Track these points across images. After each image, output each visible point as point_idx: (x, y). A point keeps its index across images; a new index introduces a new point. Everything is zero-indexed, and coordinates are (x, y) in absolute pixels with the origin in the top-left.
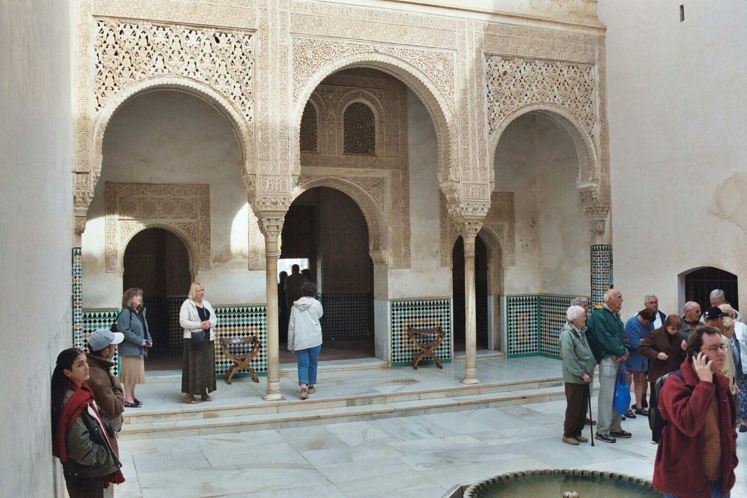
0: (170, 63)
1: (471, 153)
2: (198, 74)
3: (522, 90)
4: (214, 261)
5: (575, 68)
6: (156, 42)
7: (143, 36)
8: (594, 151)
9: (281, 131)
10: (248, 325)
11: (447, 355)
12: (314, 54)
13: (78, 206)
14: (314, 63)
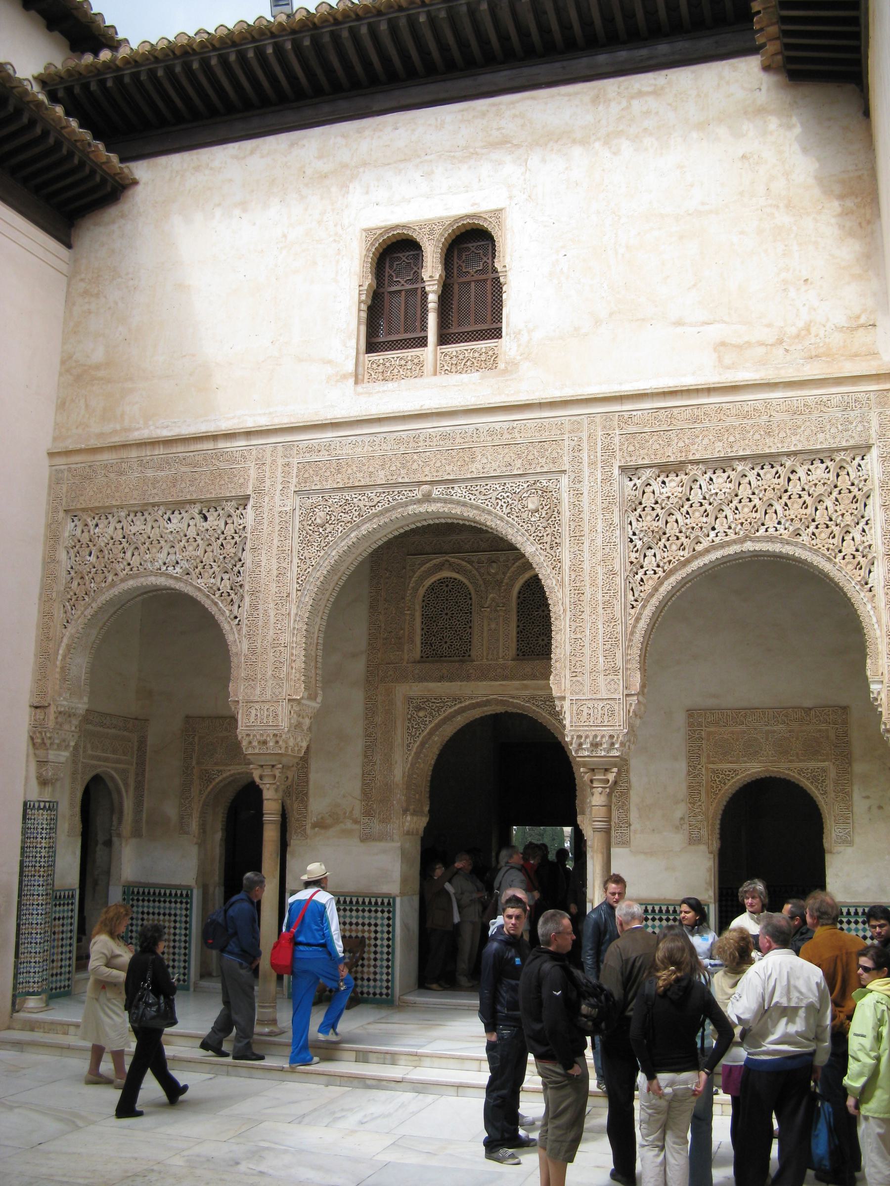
0: (148, 556)
1: (587, 645)
2: (178, 569)
4: (315, 826)
6: (133, 532)
7: (119, 526)
9: (274, 637)
10: (357, 924)
12: (328, 517)
13: (37, 749)
14: (328, 530)
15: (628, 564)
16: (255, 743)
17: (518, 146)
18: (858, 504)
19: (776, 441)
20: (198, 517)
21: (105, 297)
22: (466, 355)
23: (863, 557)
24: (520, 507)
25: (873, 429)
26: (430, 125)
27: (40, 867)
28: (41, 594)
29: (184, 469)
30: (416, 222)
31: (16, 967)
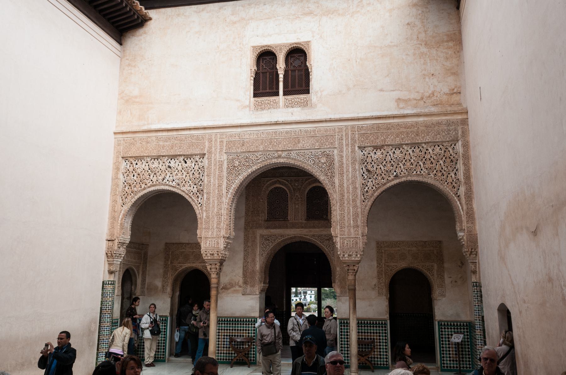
1: (346, 216)
2: (174, 183)
3: (392, 168)
4: (222, 289)
5: (441, 146)
6: (153, 167)
7: (147, 164)
8: (460, 208)
9: (217, 211)
10: (241, 330)
11: (385, 363)
12: (239, 163)
13: (109, 258)
14: (239, 169)
15: (362, 185)
16: (209, 255)
17: (316, 15)
18: (453, 163)
19: (420, 138)
20: (183, 162)
21: (138, 68)
22: (295, 100)
23: (456, 183)
24: (318, 161)
25: (460, 134)
26: (279, 4)
27: (109, 309)
28: (111, 192)
29: (176, 142)
30: (274, 44)
31: (97, 355)
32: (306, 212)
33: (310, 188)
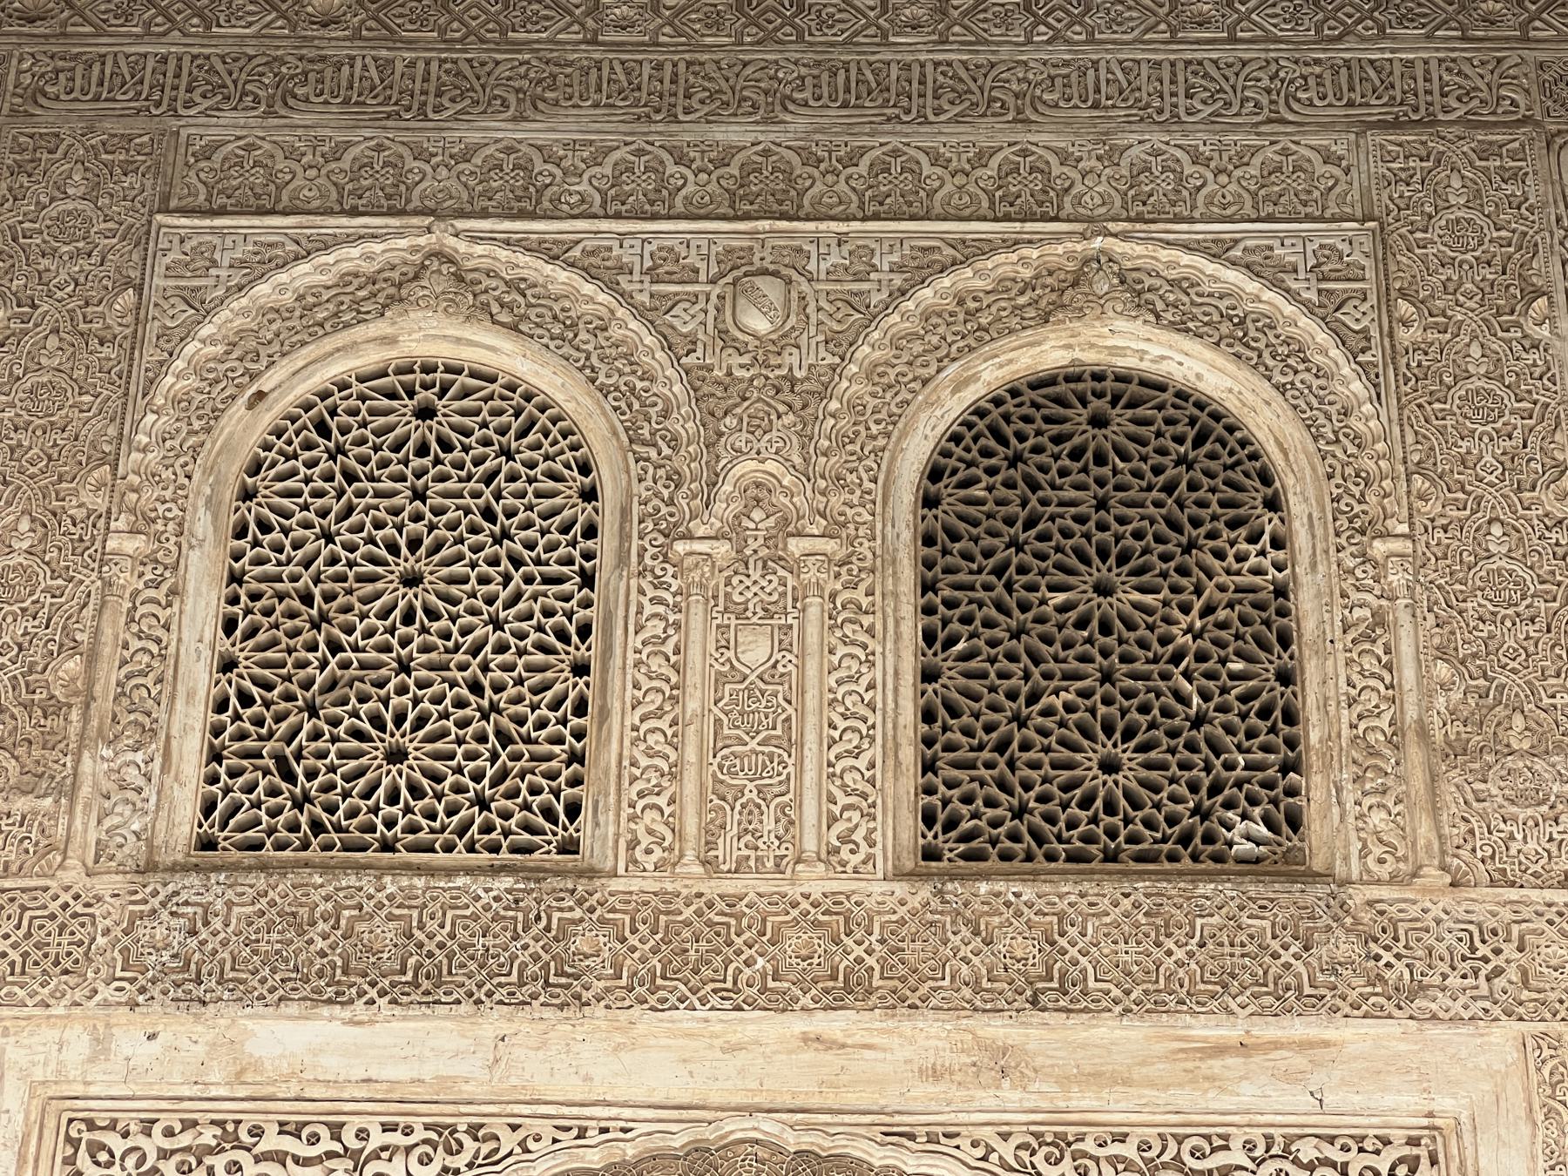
32: (909, 755)
33: (972, 394)
